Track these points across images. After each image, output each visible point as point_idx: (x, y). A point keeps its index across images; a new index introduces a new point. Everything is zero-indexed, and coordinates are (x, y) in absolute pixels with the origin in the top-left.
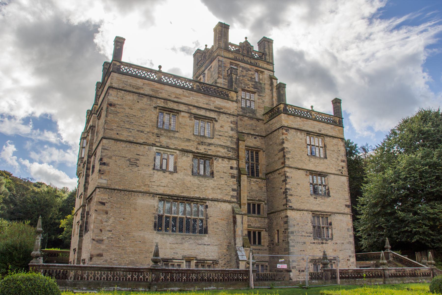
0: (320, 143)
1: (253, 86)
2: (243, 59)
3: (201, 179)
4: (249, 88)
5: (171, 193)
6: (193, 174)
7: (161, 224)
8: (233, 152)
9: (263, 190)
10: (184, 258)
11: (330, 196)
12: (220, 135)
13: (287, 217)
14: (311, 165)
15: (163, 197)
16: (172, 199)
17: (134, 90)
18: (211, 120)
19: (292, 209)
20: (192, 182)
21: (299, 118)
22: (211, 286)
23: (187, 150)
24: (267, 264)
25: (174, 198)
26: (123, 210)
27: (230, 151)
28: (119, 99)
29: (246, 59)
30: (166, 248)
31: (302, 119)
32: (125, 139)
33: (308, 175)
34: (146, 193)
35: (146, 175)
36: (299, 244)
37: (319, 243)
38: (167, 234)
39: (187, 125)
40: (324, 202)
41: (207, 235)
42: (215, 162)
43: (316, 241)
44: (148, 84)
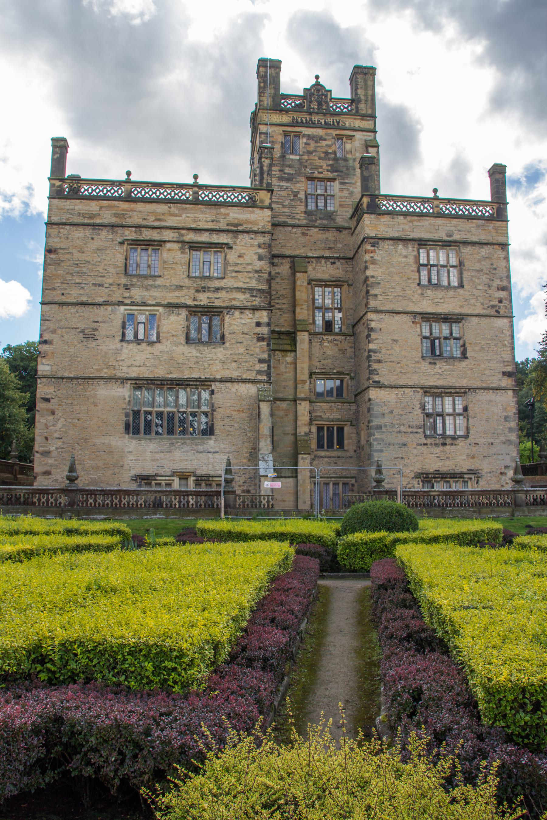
0: (441, 259)
1: (329, 168)
2: (311, 120)
3: (201, 348)
4: (322, 173)
5: (151, 376)
6: (188, 340)
7: (137, 424)
8: (260, 298)
9: (348, 355)
10: (174, 474)
11: (467, 358)
12: (236, 272)
13: (370, 400)
14: (425, 302)
15: (137, 382)
16: (154, 384)
17: (86, 221)
18: (221, 248)
19: (379, 385)
20: (186, 354)
21: (401, 217)
22: (156, 514)
23: (177, 304)
24: (353, 481)
25: (156, 382)
26: (77, 407)
27: (256, 296)
28: (63, 240)
29: (315, 118)
30: (145, 460)
31: (409, 218)
32: (75, 301)
33: (417, 323)
34: (110, 378)
35: (111, 352)
36: (391, 446)
39: (176, 263)
40: (452, 370)
41: (213, 437)
42: (227, 318)
43: (429, 441)
44: (109, 207)
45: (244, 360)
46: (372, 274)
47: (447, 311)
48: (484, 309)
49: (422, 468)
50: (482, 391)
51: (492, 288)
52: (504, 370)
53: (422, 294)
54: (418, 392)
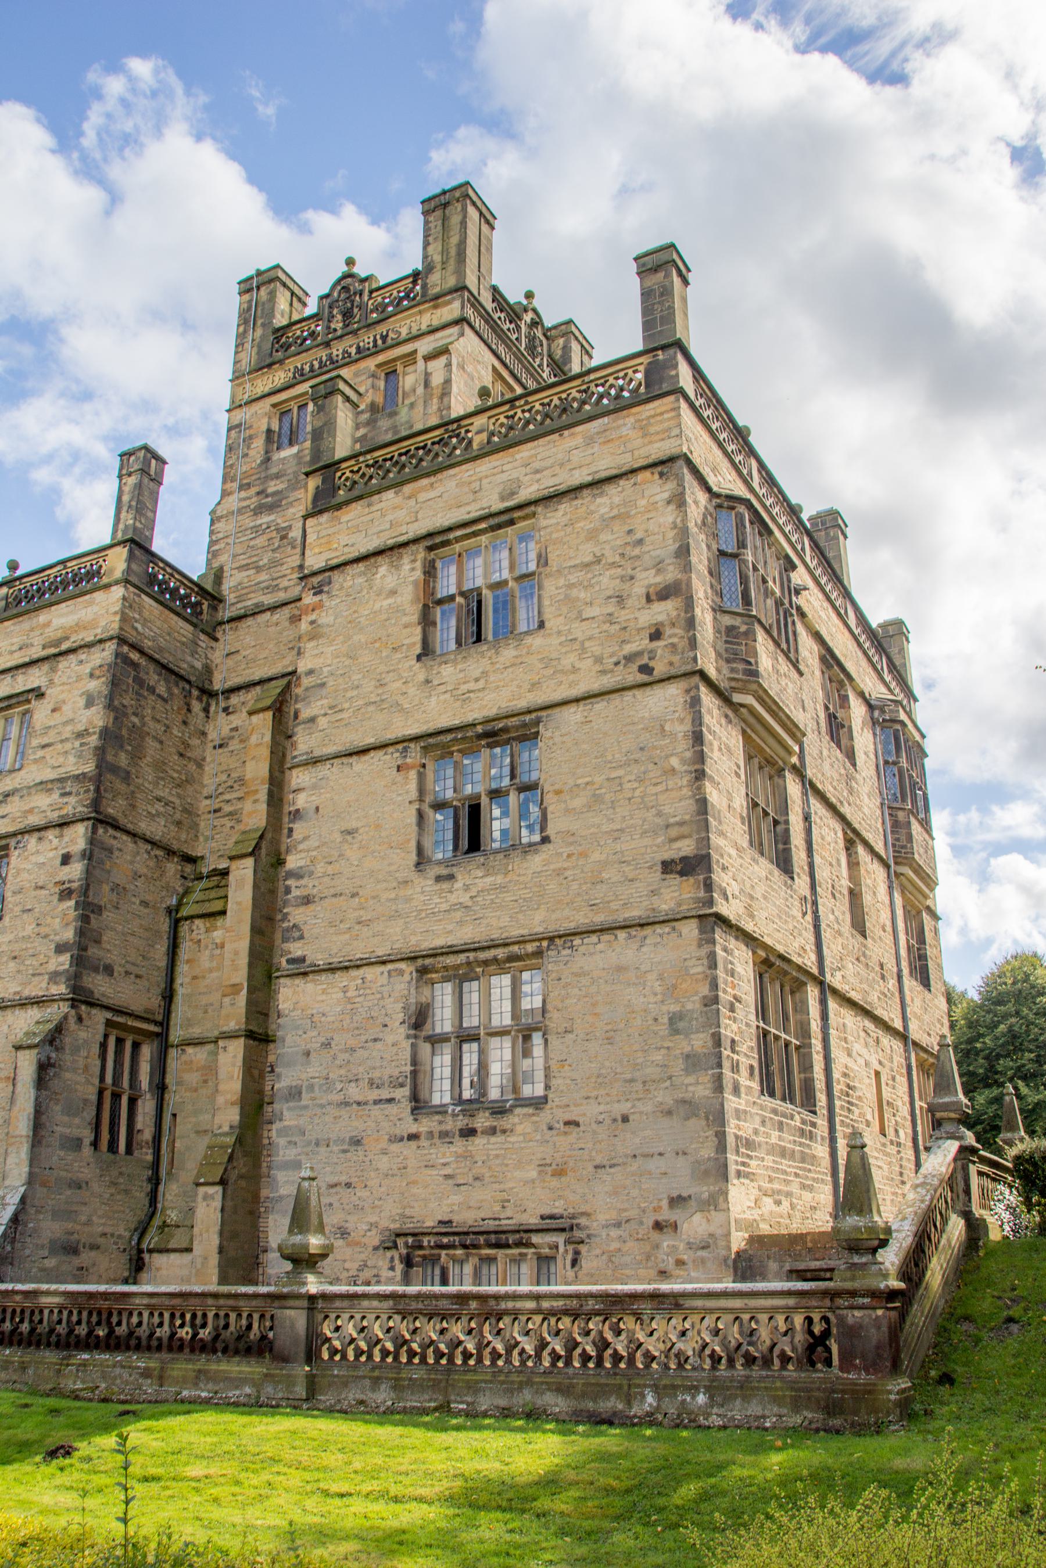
8: (78, 794)
12: (44, 747)
27: (70, 794)
31: (407, 489)
36: (323, 1149)
37: (444, 1135)
40: (503, 888)
43: (426, 1125)
45: (31, 952)
46: (310, 666)
47: (492, 712)
48: (603, 672)
49: (403, 1216)
50: (594, 938)
51: (629, 603)
52: (667, 856)
53: (428, 681)
54: (401, 973)
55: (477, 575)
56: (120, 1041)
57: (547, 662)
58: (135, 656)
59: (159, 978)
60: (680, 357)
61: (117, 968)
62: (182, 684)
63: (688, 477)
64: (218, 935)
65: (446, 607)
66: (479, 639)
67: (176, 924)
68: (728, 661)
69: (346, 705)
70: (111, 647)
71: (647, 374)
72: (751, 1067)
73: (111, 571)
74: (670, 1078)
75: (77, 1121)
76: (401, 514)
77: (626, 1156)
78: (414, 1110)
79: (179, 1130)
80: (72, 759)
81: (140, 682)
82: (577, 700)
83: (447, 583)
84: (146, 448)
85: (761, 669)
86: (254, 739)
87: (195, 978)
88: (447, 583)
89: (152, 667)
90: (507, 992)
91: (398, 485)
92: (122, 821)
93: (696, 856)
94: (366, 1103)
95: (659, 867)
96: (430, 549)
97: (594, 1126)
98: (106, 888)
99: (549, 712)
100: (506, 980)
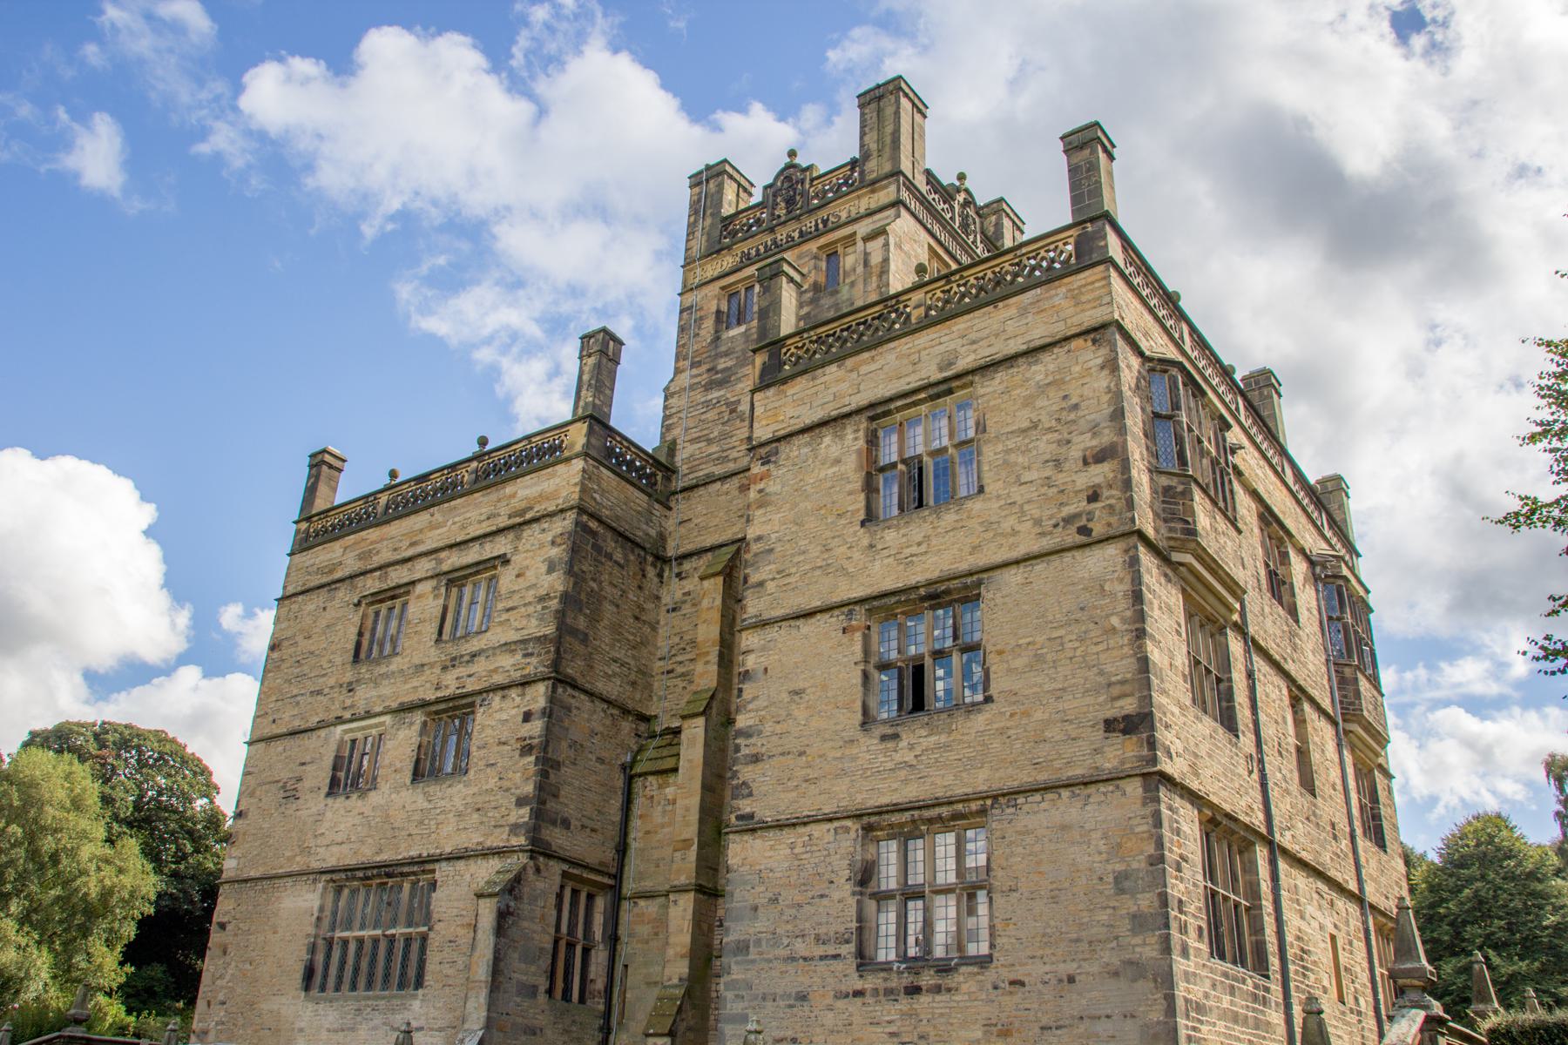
5: (351, 861)
8: (539, 655)
12: (508, 610)
27: (532, 654)
31: (849, 362)
36: (769, 1004)
37: (889, 992)
38: (325, 1000)
40: (947, 747)
43: (871, 982)
47: (935, 575)
48: (1043, 534)
50: (1038, 797)
51: (1066, 466)
52: (1109, 714)
53: (871, 546)
54: (847, 830)
55: (918, 443)
56: (575, 892)
57: (988, 525)
58: (593, 525)
59: (613, 832)
60: (1108, 228)
61: (574, 822)
62: (637, 551)
63: (1120, 343)
64: (670, 791)
65: (888, 474)
66: (920, 505)
67: (630, 780)
68: (1165, 521)
69: (793, 570)
70: (571, 516)
71: (1077, 246)
72: (1200, 928)
73: (572, 445)
74: (1116, 938)
75: (533, 969)
76: (844, 386)
77: (1073, 1017)
78: (859, 966)
79: (631, 980)
80: (534, 622)
81: (598, 549)
82: (1017, 562)
83: (890, 452)
84: (604, 330)
85: (1199, 528)
86: (705, 603)
87: (648, 832)
88: (890, 452)
89: (609, 535)
90: (952, 850)
91: (839, 359)
92: (580, 681)
93: (1138, 714)
94: (812, 959)
95: (1102, 726)
96: (872, 419)
97: (1040, 986)
98: (564, 744)
99: (991, 574)
100: (951, 838)
